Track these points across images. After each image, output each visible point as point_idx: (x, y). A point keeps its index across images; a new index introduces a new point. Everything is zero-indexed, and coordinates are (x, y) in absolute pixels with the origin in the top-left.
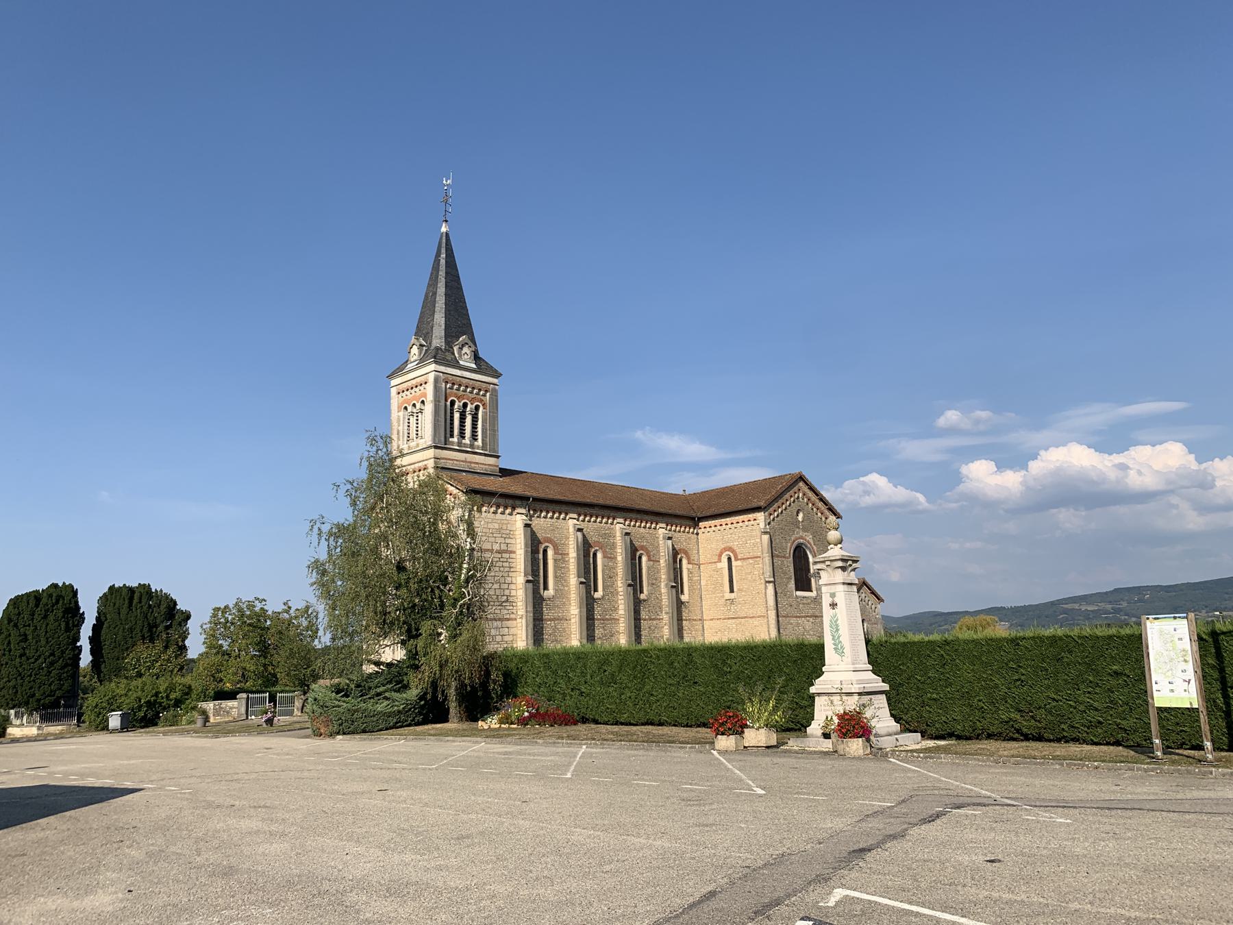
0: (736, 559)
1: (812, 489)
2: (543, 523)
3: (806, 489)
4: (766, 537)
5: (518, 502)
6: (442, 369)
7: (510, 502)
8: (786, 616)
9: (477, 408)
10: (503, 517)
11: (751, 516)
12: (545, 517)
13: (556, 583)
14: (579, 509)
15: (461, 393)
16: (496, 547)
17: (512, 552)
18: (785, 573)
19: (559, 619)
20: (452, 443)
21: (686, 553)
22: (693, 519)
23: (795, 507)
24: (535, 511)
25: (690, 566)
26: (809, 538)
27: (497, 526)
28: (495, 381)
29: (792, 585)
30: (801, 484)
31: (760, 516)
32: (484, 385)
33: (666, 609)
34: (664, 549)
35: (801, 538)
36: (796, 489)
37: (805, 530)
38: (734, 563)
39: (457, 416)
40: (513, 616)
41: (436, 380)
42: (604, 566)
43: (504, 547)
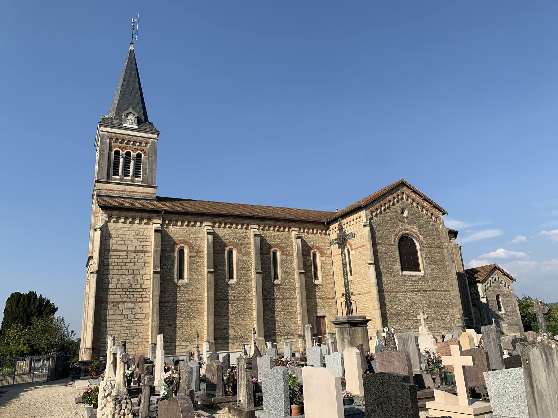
0: (352, 250)
1: (414, 192)
2: (177, 231)
3: (410, 192)
4: (368, 229)
5: (153, 215)
7: (147, 215)
8: (392, 291)
11: (357, 215)
13: (189, 274)
14: (214, 219)
15: (124, 145)
16: (133, 248)
17: (146, 252)
18: (389, 257)
19: (192, 301)
20: (115, 179)
21: (319, 249)
22: (323, 223)
23: (398, 207)
24: (170, 221)
25: (323, 258)
26: (415, 229)
27: (133, 233)
29: (398, 266)
30: (404, 189)
31: (363, 213)
32: (145, 140)
33: (298, 290)
34: (296, 244)
35: (407, 229)
36: (399, 192)
37: (409, 223)
38: (351, 253)
40: (144, 299)
42: (238, 260)
43: (139, 248)
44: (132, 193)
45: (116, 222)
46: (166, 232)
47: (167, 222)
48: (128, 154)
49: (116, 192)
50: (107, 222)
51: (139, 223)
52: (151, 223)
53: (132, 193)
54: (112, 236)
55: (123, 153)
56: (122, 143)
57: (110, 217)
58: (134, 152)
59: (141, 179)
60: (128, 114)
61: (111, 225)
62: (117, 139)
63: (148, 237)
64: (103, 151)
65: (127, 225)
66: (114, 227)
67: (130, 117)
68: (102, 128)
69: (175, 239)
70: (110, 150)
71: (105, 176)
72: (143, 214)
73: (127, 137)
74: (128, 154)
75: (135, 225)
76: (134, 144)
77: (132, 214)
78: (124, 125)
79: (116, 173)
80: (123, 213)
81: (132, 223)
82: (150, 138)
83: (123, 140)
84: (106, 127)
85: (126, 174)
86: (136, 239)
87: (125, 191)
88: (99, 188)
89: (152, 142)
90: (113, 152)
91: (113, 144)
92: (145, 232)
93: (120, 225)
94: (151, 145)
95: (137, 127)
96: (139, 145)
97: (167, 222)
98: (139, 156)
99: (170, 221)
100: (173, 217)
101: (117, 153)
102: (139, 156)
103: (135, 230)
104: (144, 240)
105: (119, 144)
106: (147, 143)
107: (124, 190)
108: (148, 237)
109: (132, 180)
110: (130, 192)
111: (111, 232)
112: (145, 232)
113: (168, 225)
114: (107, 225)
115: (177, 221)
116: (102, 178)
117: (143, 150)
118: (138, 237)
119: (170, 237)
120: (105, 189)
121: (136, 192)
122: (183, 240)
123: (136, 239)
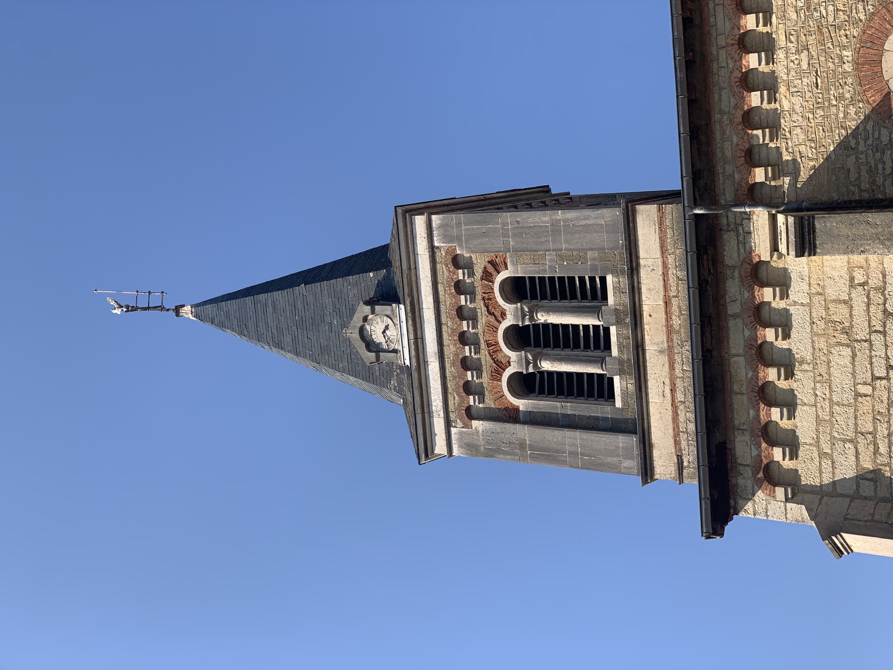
5: (730, 254)
10: (798, 317)
12: (769, 85)
15: (484, 356)
24: (752, 156)
32: (443, 271)
44: (676, 322)
45: (791, 444)
46: (817, 170)
47: (759, 175)
48: (520, 337)
50: (797, 491)
51: (784, 324)
52: (777, 263)
53: (676, 322)
54: (868, 465)
55: (515, 361)
56: (477, 368)
57: (771, 476)
58: (503, 314)
60: (370, 345)
61: (810, 470)
62: (468, 388)
63: (859, 278)
64: (522, 445)
65: (802, 385)
66: (822, 455)
67: (376, 330)
68: (440, 447)
69: (853, 116)
70: (511, 416)
72: (733, 308)
73: (450, 349)
74: (520, 337)
75: (799, 343)
76: (473, 318)
77: (739, 366)
79: (601, 388)
80: (742, 409)
81: (787, 364)
82: (432, 249)
83: (465, 364)
84: (433, 435)
85: (598, 341)
86: (877, 339)
87: (670, 348)
88: (673, 469)
89: (446, 238)
91: (490, 402)
92: (831, 293)
93: (803, 424)
94: (459, 239)
96: (470, 292)
97: (759, 175)
98: (518, 289)
99: (752, 156)
100: (727, 143)
103: (821, 344)
104: (877, 298)
105: (485, 379)
106: (456, 262)
107: (665, 359)
108: (859, 278)
110: (670, 330)
111: (846, 470)
112: (831, 293)
113: (778, 167)
114: (812, 490)
115: (750, 119)
117: (487, 276)
118: (861, 333)
119: (843, 146)
120: (677, 443)
121: (667, 303)
122: (857, 65)
123: (877, 339)
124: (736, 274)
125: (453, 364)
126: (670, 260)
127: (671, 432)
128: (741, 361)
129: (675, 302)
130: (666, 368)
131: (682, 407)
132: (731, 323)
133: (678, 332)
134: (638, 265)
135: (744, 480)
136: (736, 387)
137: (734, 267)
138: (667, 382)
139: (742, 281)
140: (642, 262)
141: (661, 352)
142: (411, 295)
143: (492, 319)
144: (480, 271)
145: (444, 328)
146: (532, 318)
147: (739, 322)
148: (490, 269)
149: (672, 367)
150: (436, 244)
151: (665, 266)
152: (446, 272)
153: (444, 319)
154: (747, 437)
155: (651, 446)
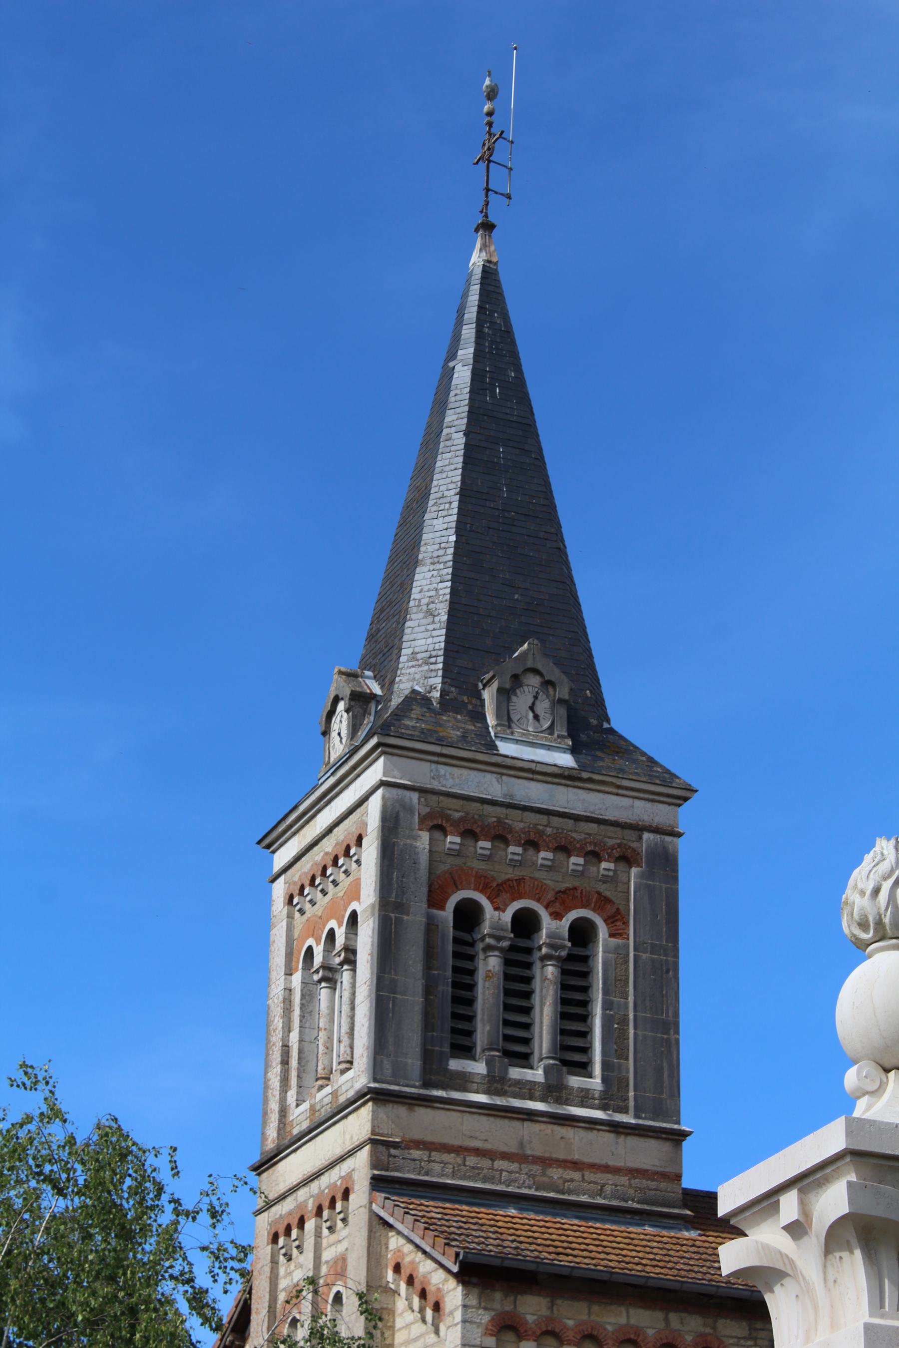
6: (421, 772)
9: (582, 934)
20: (463, 1081)
28: (658, 814)
39: (491, 965)
41: (391, 824)
44: (556, 1173)
49: (472, 1161)
55: (496, 918)
58: (557, 916)
59: (596, 1082)
71: (414, 1063)
78: (505, 748)
82: (638, 828)
90: (447, 914)
95: (566, 760)
101: (468, 916)
102: (582, 934)
107: (513, 1148)
109: (553, 1090)
110: (546, 1162)
116: (398, 1074)
117: (601, 903)
121: (576, 1165)
124: (708, 1330)
125: (500, 822)
126: (624, 1180)
127: (429, 1138)
128: (623, 1320)
129: (577, 1175)
130: (503, 1148)
131: (459, 1160)
132: (659, 1315)
133: (544, 1174)
134: (618, 1133)
135: (500, 1302)
136: (595, 1308)
137: (714, 1328)
138: (488, 1146)
139: (702, 1335)
140: (622, 1139)
141: (521, 1145)
142: (590, 780)
143: (550, 896)
144: (608, 894)
145: (543, 819)
146: (548, 957)
147: (661, 1325)
148: (610, 910)
149: (505, 1156)
150: (646, 836)
151: (615, 1171)
152: (610, 842)
153: (556, 821)
154: (545, 1312)
155: (411, 1106)
